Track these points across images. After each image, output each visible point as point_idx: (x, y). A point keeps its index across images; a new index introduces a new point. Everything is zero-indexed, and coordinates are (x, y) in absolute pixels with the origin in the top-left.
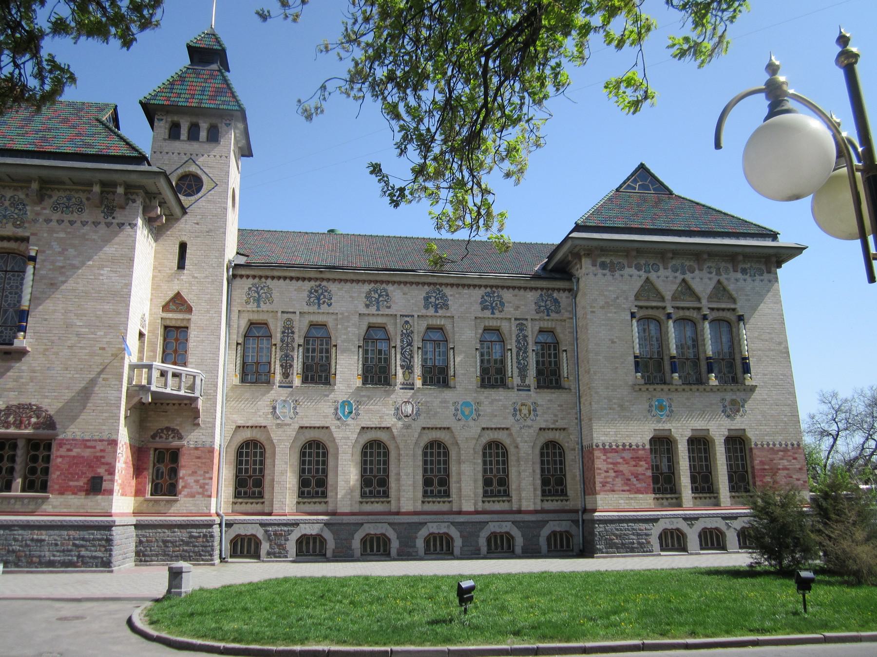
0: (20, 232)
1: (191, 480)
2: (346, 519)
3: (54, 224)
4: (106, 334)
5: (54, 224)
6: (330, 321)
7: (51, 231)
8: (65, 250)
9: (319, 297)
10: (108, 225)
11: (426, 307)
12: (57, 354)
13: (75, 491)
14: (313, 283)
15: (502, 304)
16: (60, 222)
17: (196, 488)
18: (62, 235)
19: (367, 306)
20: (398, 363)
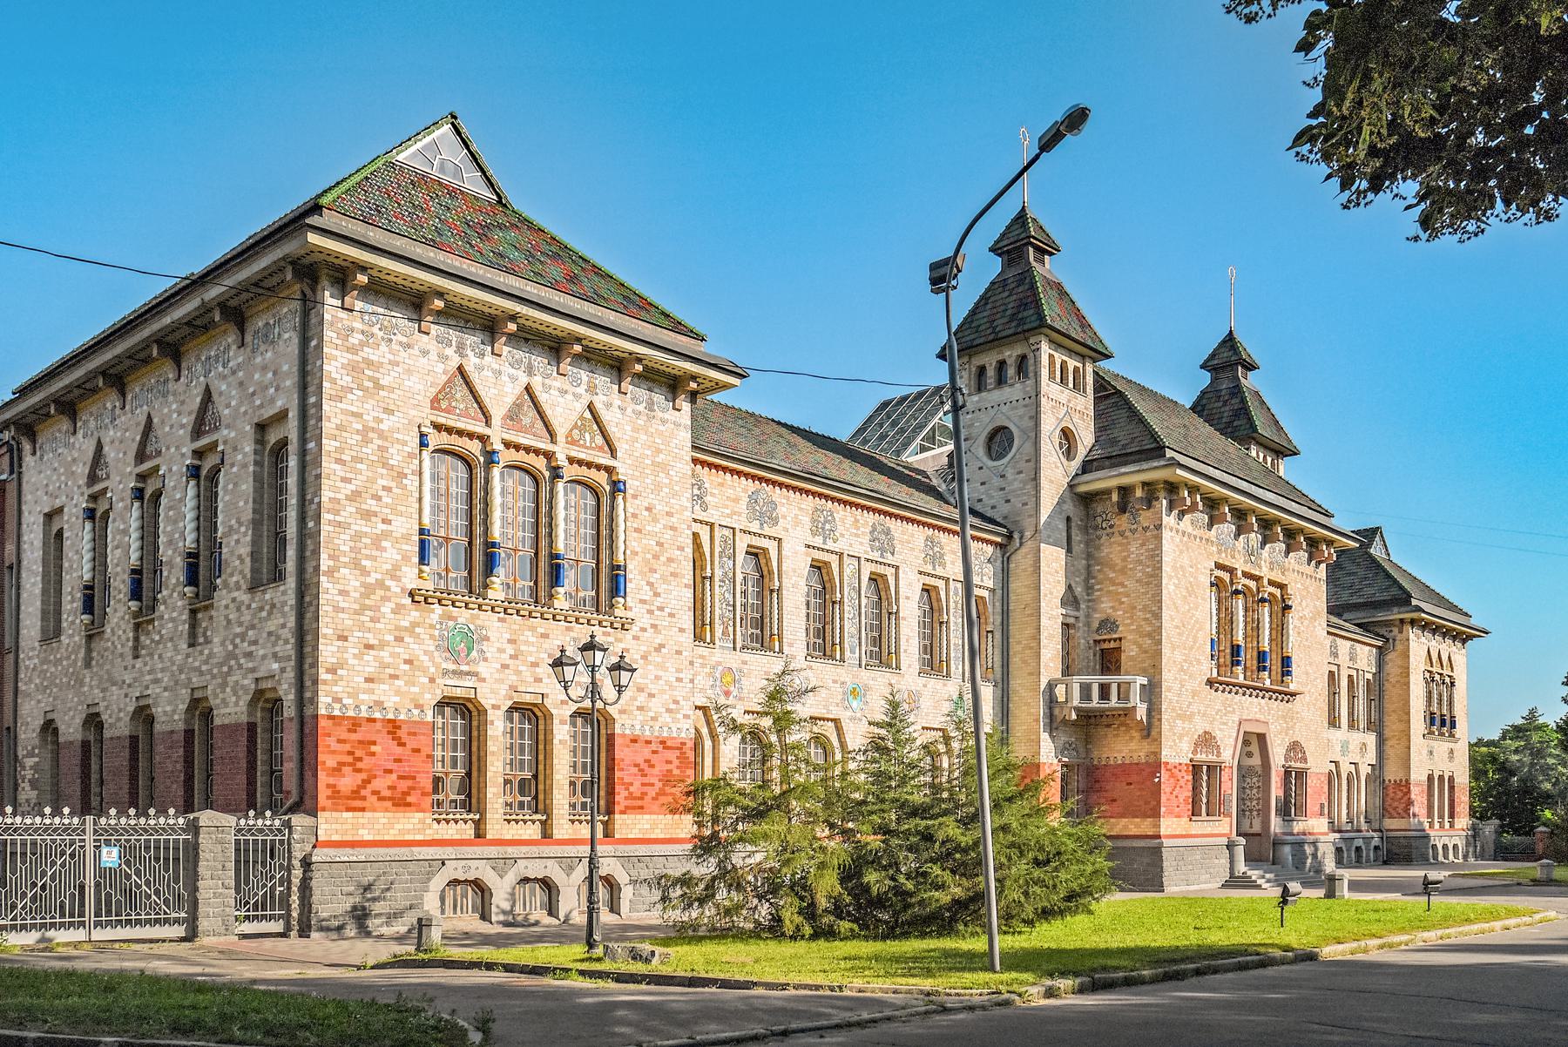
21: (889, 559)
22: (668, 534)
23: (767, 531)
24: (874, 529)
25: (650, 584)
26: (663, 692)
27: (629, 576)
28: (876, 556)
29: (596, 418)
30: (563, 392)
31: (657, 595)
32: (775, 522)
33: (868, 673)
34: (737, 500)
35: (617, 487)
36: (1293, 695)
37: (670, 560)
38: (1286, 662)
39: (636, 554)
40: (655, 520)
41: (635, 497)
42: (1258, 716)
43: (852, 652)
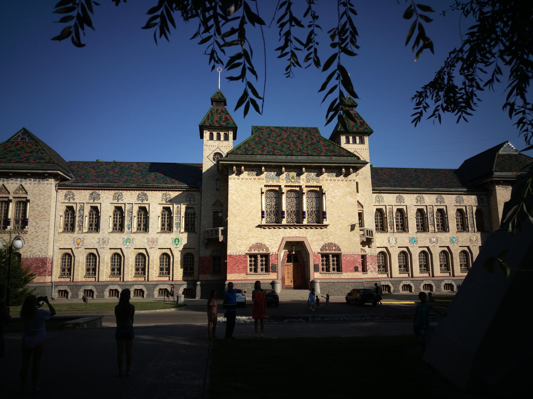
0: (319, 184)
1: (371, 266)
2: (417, 279)
3: (329, 181)
4: (352, 219)
5: (329, 181)
6: (404, 208)
7: (329, 184)
8: (334, 190)
9: (400, 200)
10: (346, 181)
11: (437, 202)
12: (337, 226)
13: (351, 271)
14: (397, 195)
15: (463, 200)
16: (331, 180)
17: (373, 269)
18: (332, 185)
19: (417, 202)
20: (429, 223)
21: (145, 202)
22: (43, 210)
23: (96, 201)
24: (139, 194)
25: (36, 222)
26: (37, 247)
27: (29, 221)
28: (140, 202)
29: (23, 187)
30: (12, 184)
31: (37, 224)
32: (99, 199)
33: (134, 235)
34: (86, 196)
35: (29, 201)
36: (326, 226)
37: (43, 215)
38: (324, 214)
39: (31, 215)
40: (39, 207)
41: (32, 203)
42: (297, 235)
43: (129, 229)
